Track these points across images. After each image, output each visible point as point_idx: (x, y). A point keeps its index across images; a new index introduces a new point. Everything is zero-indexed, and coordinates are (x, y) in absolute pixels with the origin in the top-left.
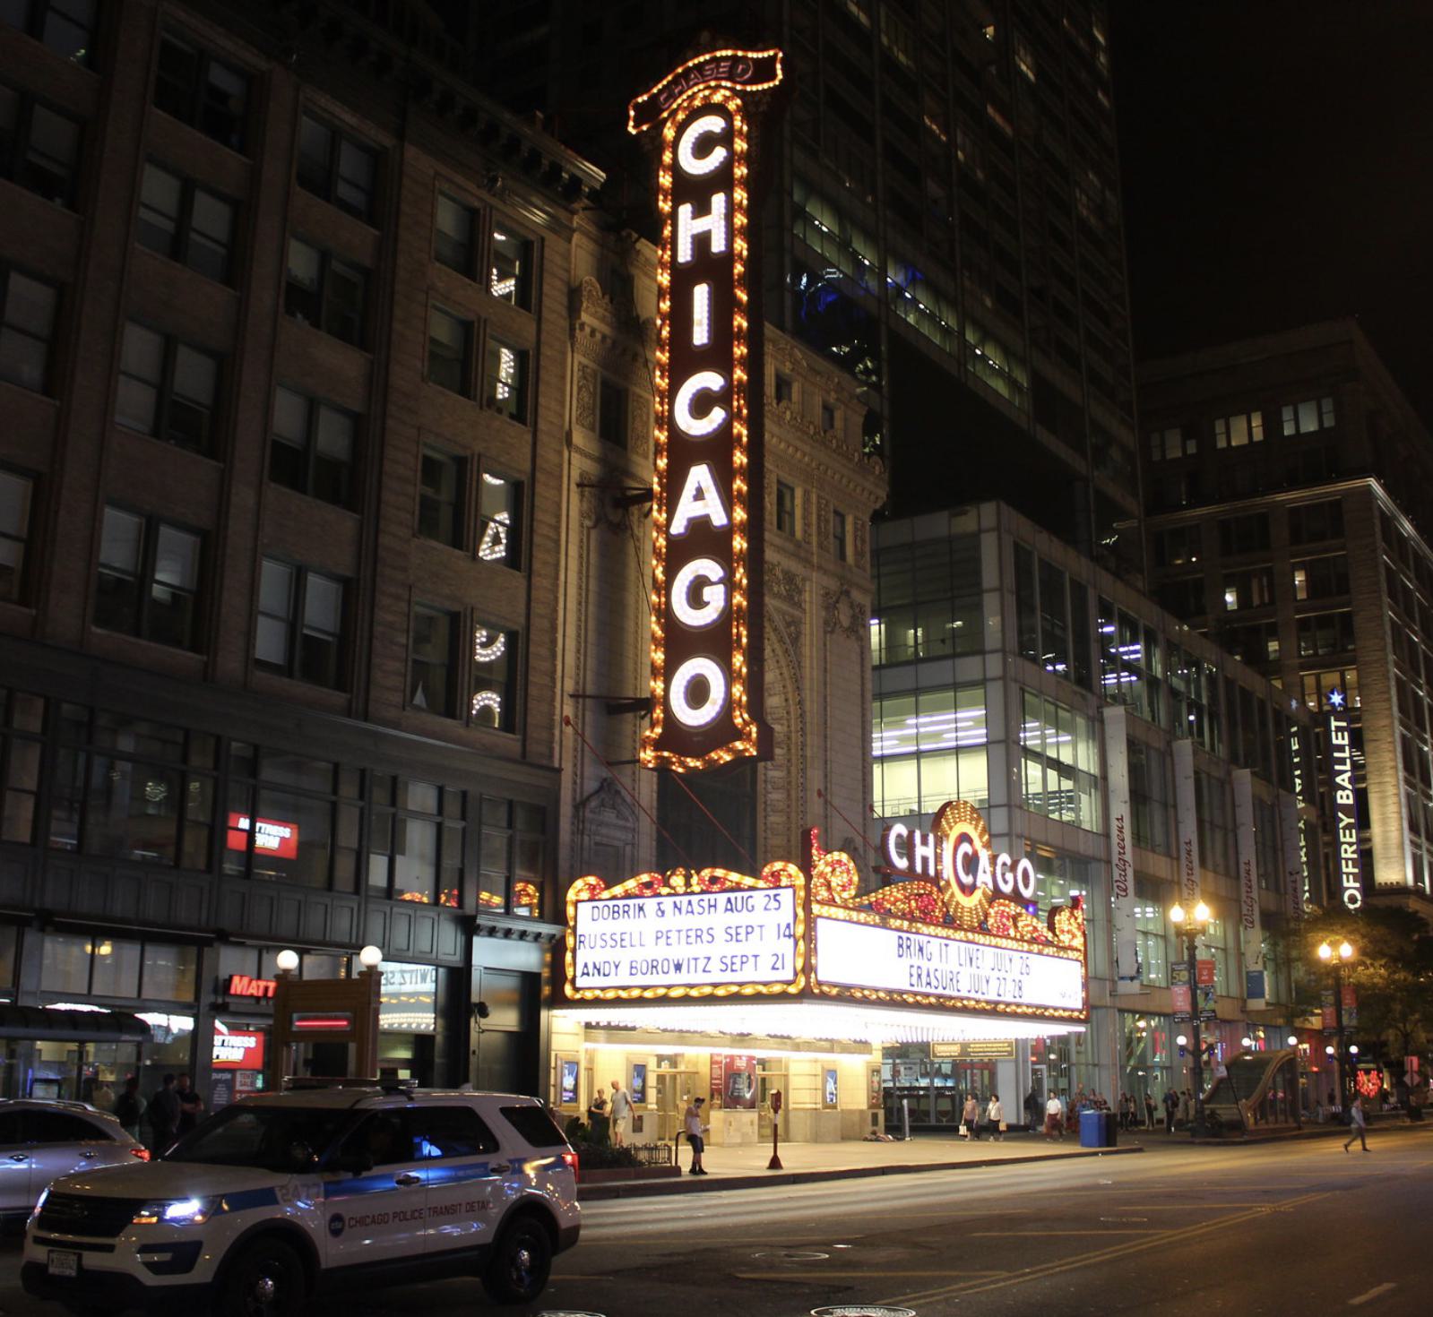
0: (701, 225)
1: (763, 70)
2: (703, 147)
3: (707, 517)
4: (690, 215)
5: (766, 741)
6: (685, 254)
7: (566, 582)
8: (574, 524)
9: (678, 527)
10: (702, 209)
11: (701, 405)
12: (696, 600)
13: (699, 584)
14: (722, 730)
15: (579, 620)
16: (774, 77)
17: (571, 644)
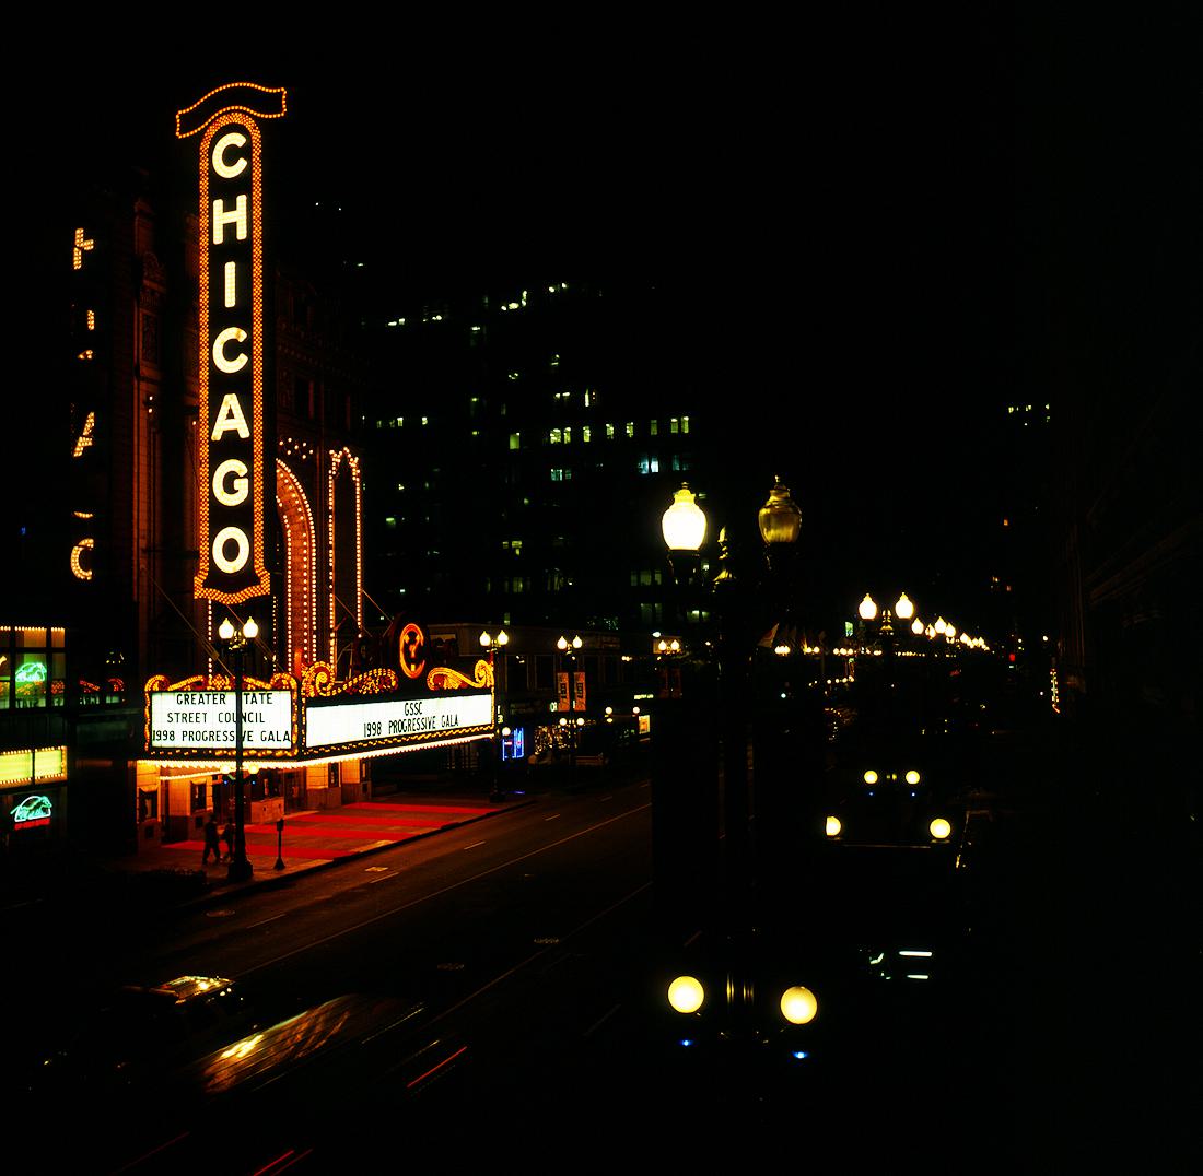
0: (230, 217)
1: (271, 103)
2: (231, 156)
3: (236, 431)
4: (222, 207)
5: (278, 584)
6: (218, 238)
7: (138, 473)
8: (143, 432)
9: (217, 435)
10: (230, 206)
11: (232, 350)
12: (229, 487)
13: (230, 478)
14: (247, 577)
15: (149, 480)
16: (280, 111)
17: (144, 516)
